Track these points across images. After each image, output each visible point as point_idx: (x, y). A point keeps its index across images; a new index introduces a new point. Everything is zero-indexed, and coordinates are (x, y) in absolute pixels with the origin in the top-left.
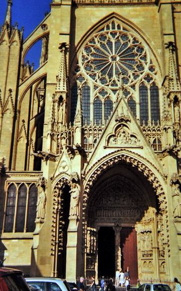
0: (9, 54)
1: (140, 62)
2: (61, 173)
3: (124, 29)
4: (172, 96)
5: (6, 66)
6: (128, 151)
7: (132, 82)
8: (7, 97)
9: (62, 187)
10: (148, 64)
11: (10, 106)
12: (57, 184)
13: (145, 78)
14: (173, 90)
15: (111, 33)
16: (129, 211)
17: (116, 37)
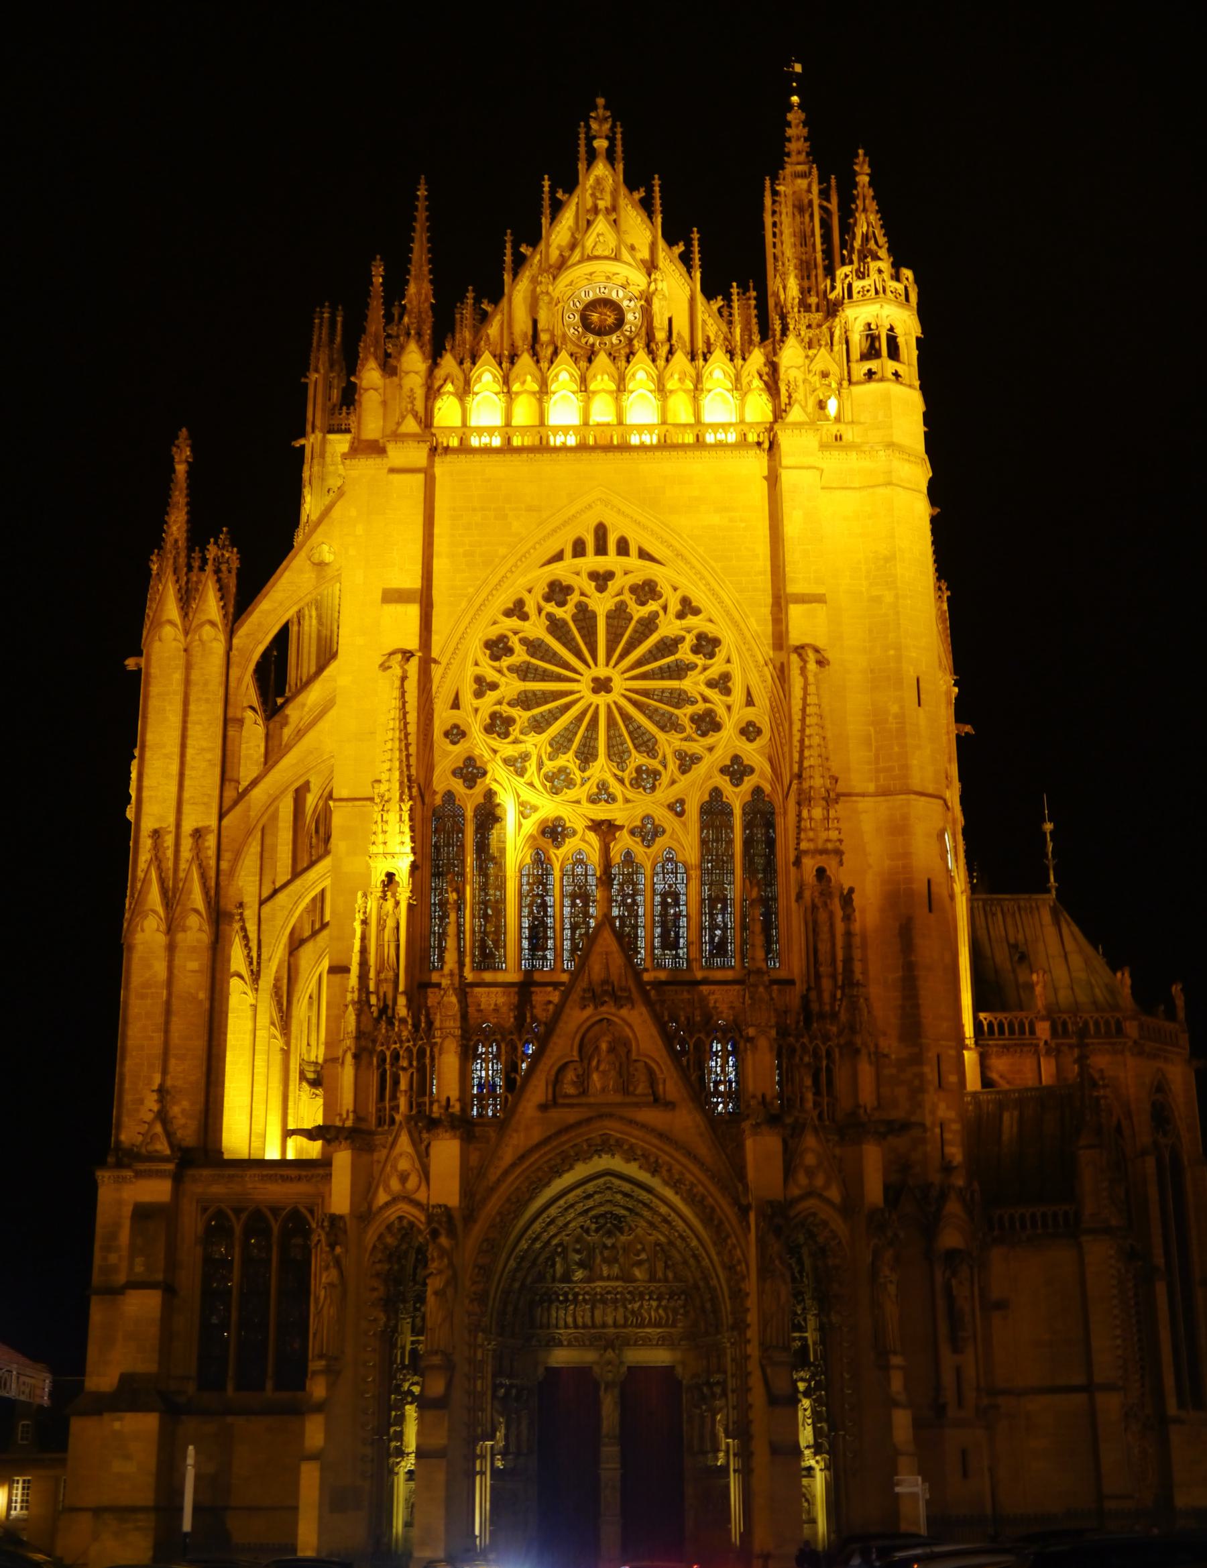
0: (187, 682)
1: (705, 700)
2: (395, 1200)
3: (644, 555)
4: (809, 864)
5: (176, 734)
6: (622, 1118)
7: (673, 782)
8: (183, 865)
9: (397, 1247)
10: (735, 709)
11: (197, 898)
12: (381, 1237)
13: (724, 771)
14: (811, 846)
15: (594, 576)
16: (654, 1304)
17: (613, 586)
